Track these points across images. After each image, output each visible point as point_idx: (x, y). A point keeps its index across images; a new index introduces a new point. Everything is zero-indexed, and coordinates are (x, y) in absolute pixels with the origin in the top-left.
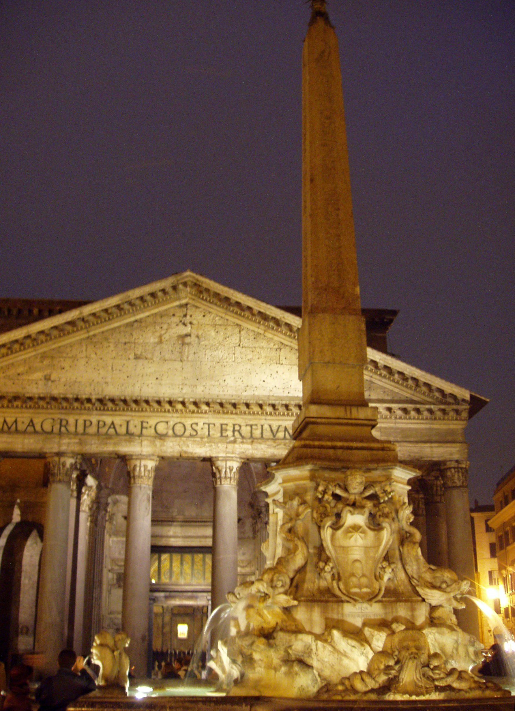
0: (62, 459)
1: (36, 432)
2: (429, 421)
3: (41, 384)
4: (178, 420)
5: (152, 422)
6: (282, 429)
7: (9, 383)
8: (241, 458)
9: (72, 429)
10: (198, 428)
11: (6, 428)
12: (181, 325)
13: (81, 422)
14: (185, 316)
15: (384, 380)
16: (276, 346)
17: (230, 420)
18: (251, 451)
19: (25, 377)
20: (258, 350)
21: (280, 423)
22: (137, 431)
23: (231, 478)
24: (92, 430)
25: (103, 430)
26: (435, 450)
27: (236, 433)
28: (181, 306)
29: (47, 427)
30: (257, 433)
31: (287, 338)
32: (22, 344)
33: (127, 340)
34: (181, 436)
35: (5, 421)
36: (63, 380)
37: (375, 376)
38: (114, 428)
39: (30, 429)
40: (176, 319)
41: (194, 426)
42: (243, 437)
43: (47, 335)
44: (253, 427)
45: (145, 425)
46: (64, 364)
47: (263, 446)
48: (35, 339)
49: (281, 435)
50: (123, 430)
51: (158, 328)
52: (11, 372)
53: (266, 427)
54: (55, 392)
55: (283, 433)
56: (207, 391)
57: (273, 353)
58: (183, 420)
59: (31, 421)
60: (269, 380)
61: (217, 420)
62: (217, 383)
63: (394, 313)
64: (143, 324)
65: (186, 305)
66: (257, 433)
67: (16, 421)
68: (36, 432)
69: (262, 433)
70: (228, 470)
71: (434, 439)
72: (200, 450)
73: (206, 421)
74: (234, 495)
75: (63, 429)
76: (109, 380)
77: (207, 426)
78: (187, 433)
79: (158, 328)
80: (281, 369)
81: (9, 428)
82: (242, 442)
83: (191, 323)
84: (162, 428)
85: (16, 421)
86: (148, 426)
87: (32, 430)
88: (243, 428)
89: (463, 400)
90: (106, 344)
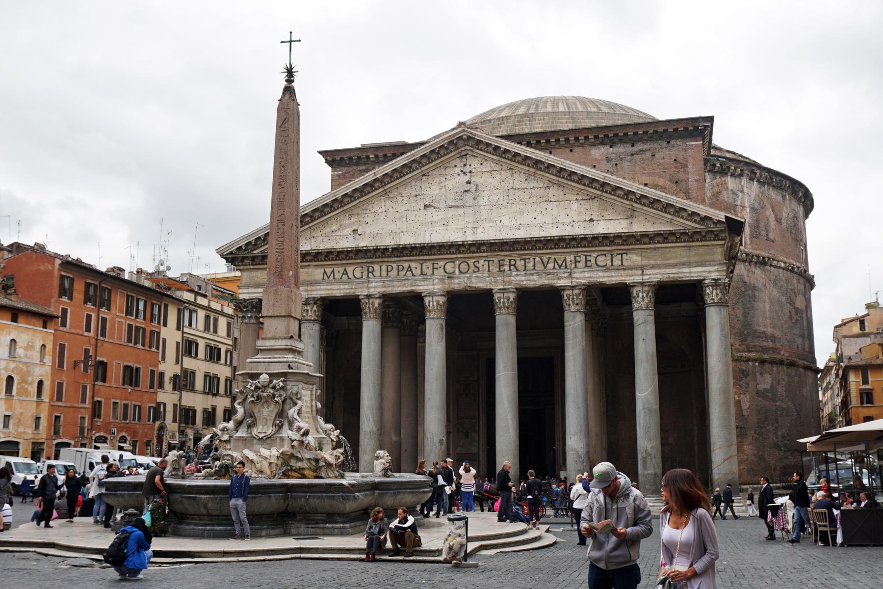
0: (371, 301)
3: (351, 238)
6: (552, 260)
7: (326, 239)
8: (516, 289)
9: (377, 274)
10: (480, 265)
13: (384, 267)
14: (465, 165)
15: (644, 208)
18: (525, 283)
19: (337, 233)
20: (529, 190)
21: (548, 256)
23: (508, 308)
26: (693, 270)
29: (358, 274)
30: (530, 265)
31: (555, 178)
32: (331, 207)
36: (368, 233)
37: (636, 205)
38: (411, 271)
39: (345, 277)
40: (458, 170)
43: (351, 197)
47: (535, 277)
48: (342, 202)
49: (551, 266)
50: (419, 271)
51: (443, 179)
52: (327, 230)
53: (538, 259)
54: (363, 243)
56: (486, 231)
57: (542, 192)
60: (539, 217)
62: (494, 224)
63: (711, 119)
66: (530, 265)
67: (333, 271)
69: (534, 265)
71: (693, 259)
72: (482, 285)
74: (512, 320)
75: (370, 275)
76: (404, 230)
77: (486, 263)
78: (470, 271)
79: (443, 179)
80: (550, 206)
82: (517, 275)
83: (471, 172)
85: (333, 271)
88: (518, 262)
89: (719, 222)
90: (400, 198)
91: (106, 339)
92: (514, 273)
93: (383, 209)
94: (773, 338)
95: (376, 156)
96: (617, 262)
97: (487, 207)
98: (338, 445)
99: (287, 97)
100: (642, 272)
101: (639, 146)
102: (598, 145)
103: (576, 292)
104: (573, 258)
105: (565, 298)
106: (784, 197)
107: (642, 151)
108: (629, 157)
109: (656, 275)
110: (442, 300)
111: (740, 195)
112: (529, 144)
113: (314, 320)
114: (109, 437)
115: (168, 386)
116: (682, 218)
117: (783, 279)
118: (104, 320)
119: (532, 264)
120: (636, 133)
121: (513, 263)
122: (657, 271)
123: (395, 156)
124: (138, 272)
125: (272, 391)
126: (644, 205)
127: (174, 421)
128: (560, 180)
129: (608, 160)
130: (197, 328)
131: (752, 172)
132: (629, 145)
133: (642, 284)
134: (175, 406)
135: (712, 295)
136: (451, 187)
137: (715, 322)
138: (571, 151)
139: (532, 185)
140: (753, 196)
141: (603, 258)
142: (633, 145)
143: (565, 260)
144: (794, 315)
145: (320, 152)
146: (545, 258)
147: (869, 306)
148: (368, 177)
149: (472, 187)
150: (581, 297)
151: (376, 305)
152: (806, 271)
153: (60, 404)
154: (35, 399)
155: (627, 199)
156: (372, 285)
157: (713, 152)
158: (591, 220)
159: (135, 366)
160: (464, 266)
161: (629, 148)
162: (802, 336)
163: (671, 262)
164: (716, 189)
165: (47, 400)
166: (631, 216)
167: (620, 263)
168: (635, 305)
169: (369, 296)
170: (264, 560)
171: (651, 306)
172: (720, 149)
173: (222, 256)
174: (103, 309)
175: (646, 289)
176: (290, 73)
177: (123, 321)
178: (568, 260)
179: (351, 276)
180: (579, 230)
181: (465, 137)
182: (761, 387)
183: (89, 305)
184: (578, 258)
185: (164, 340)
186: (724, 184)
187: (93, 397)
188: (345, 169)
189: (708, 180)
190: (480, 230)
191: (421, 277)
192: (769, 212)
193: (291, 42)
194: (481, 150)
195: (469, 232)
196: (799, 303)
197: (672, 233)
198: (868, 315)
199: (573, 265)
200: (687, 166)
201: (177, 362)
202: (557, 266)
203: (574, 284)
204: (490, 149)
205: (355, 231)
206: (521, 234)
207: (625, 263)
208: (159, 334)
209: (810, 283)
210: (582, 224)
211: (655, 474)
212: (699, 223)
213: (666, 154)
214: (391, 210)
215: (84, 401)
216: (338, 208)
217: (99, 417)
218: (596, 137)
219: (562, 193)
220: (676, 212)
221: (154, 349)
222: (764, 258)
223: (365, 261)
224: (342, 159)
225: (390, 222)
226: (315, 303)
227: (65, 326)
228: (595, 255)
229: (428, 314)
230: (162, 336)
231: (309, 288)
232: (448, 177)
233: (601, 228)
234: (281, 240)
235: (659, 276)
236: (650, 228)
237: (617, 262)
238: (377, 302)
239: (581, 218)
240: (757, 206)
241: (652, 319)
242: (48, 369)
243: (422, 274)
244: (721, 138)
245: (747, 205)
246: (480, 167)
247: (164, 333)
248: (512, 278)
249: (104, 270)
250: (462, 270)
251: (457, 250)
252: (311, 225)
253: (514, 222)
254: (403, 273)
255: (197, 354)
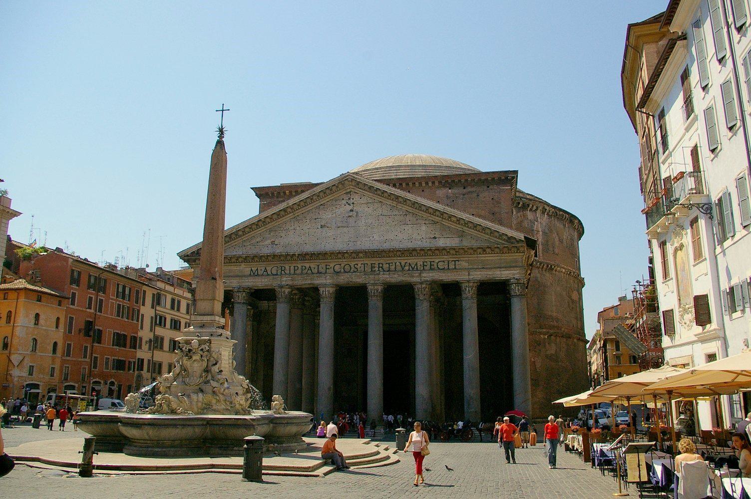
0: (283, 290)
1: (268, 275)
2: (500, 255)
4: (347, 263)
5: (332, 265)
9: (288, 272)
10: (358, 267)
11: (252, 273)
12: (347, 205)
13: (292, 268)
14: (349, 199)
15: (471, 230)
16: (404, 213)
17: (376, 261)
22: (323, 271)
24: (299, 272)
25: (305, 271)
26: (503, 272)
27: (380, 269)
28: (347, 193)
29: (274, 272)
30: (393, 268)
31: (410, 208)
33: (316, 217)
34: (347, 272)
35: (251, 270)
40: (344, 202)
41: (356, 266)
42: (384, 271)
44: (390, 264)
45: (328, 267)
46: (283, 235)
47: (396, 276)
48: (264, 222)
49: (407, 268)
51: (334, 208)
52: (254, 241)
53: (398, 264)
54: (278, 251)
55: (408, 267)
56: (363, 243)
57: (402, 218)
58: (349, 263)
59: (266, 269)
61: (369, 261)
62: (368, 239)
63: (516, 172)
64: (326, 206)
65: (350, 192)
66: (393, 268)
67: (257, 269)
68: (268, 275)
69: (395, 268)
70: (375, 291)
73: (362, 262)
74: (380, 304)
79: (334, 208)
80: (406, 227)
81: (254, 274)
82: (384, 274)
83: (353, 204)
84: (337, 268)
85: (257, 269)
86: (330, 267)
87: (266, 274)
91: (102, 314)
92: (381, 273)
93: (293, 227)
94: (557, 320)
95: (290, 192)
96: (452, 266)
97: (364, 227)
98: (248, 391)
99: (218, 147)
100: (469, 274)
101: (469, 189)
102: (441, 187)
103: (424, 286)
104: (422, 263)
105: (417, 290)
106: (565, 226)
107: (469, 192)
108: (462, 196)
109: (480, 275)
110: (332, 290)
111: (536, 223)
112: (394, 186)
113: (243, 303)
114: (102, 382)
115: (145, 347)
116: (496, 237)
117: (564, 280)
118: (101, 301)
119: (394, 267)
120: (466, 180)
121: (381, 265)
122: (479, 273)
123: (303, 191)
124: (126, 268)
125: (201, 353)
126: (470, 228)
127: (148, 371)
128: (414, 210)
129: (448, 197)
130: (165, 308)
131: (544, 208)
132: (462, 188)
133: (468, 281)
134: (149, 361)
135: (515, 289)
136: (339, 213)
137: (518, 309)
138: (423, 191)
139: (395, 213)
140: (544, 224)
141: (443, 263)
142: (465, 188)
143: (416, 264)
144: (571, 304)
145: (252, 188)
146: (403, 264)
147: (620, 299)
148: (283, 206)
149: (354, 213)
150: (427, 290)
151: (287, 293)
152: (579, 275)
153: (68, 358)
154: (51, 355)
155: (459, 224)
156: (283, 281)
157: (517, 194)
158: (435, 238)
159: (122, 333)
160: (347, 267)
161: (461, 190)
162: (576, 318)
163: (489, 267)
164: (520, 219)
165: (60, 356)
166: (462, 235)
167: (454, 267)
168: (464, 296)
169: (281, 287)
170: (185, 473)
171: (475, 296)
172: (522, 192)
173: (181, 258)
174: (101, 294)
175: (471, 284)
176: (221, 131)
177: (114, 302)
178: (419, 265)
179: (269, 273)
180: (426, 244)
181: (349, 179)
182: (548, 353)
183: (91, 291)
184: (425, 263)
185: (143, 315)
186: (525, 216)
187: (92, 354)
188: (269, 200)
189: (514, 213)
190: (359, 243)
191: (318, 275)
192: (555, 235)
193: (223, 111)
194: (360, 189)
195: (351, 244)
196: (575, 296)
197: (488, 247)
198: (620, 305)
199: (422, 268)
200: (500, 203)
201: (151, 330)
202: (411, 269)
203: (423, 280)
204: (366, 188)
205: (273, 243)
206: (386, 246)
207: (457, 267)
208: (139, 311)
209: (581, 283)
210: (428, 240)
211: (476, 412)
212: (507, 241)
213: (486, 195)
214: (298, 228)
215: (85, 357)
216: (262, 226)
217: (95, 367)
218: (440, 182)
219: (415, 219)
220: (491, 233)
221: (135, 322)
222: (551, 266)
223: (279, 263)
224: (267, 194)
225: (298, 236)
226: (244, 291)
227: (74, 305)
228: (437, 261)
229: (322, 300)
230: (141, 312)
231: (240, 281)
232: (338, 206)
233: (441, 243)
234: (211, 246)
235: (480, 276)
236: (475, 244)
237: (452, 266)
238: (287, 291)
239: (427, 236)
240: (547, 231)
241: (475, 305)
242: (61, 334)
243: (318, 272)
244: (524, 185)
245: (540, 230)
246: (360, 201)
247: (143, 310)
248: (381, 276)
249: (101, 265)
250: (346, 270)
251: (343, 256)
252: (242, 238)
253: (382, 238)
254: (305, 271)
255: (165, 326)
